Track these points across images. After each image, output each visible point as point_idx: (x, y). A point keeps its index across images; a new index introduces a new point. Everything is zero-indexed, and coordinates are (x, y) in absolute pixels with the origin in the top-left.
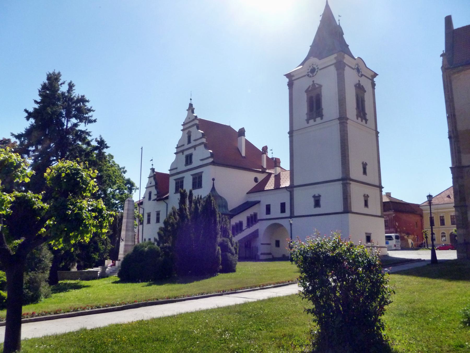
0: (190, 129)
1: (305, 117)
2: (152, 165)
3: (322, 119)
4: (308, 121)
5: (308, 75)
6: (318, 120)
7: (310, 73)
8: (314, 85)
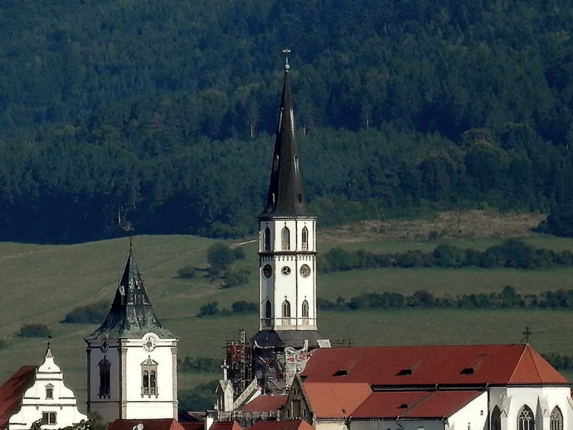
0: (52, 382)
1: (140, 391)
3: (157, 398)
4: (142, 396)
6: (153, 398)
7: (146, 346)
8: (149, 360)
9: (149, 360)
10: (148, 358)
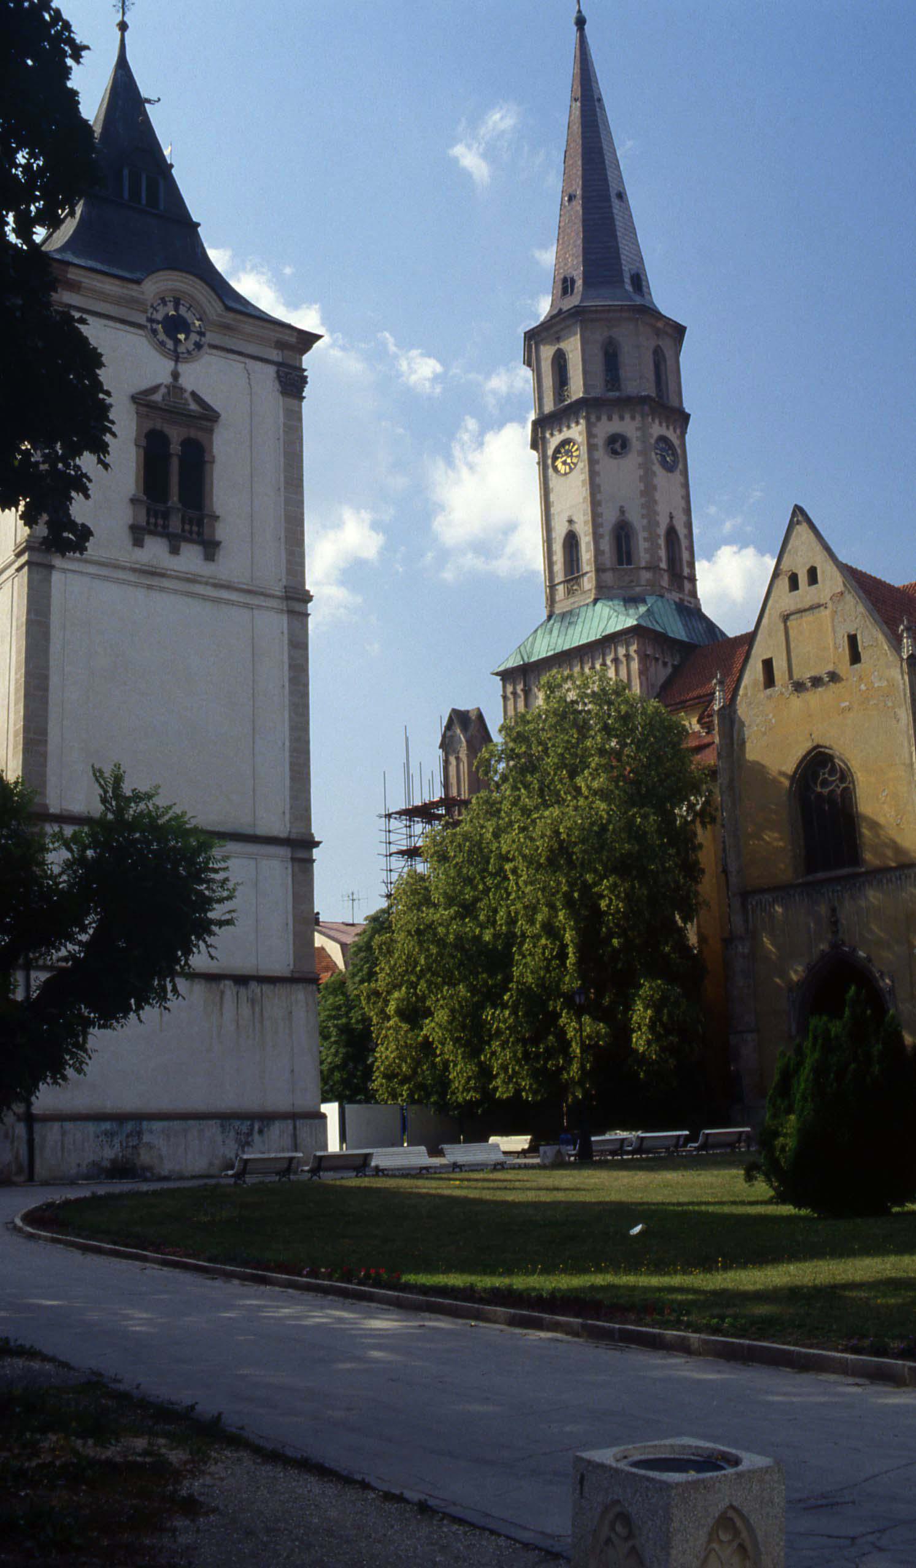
5: (154, 332)
6: (190, 559)
9: (175, 388)
10: (167, 380)
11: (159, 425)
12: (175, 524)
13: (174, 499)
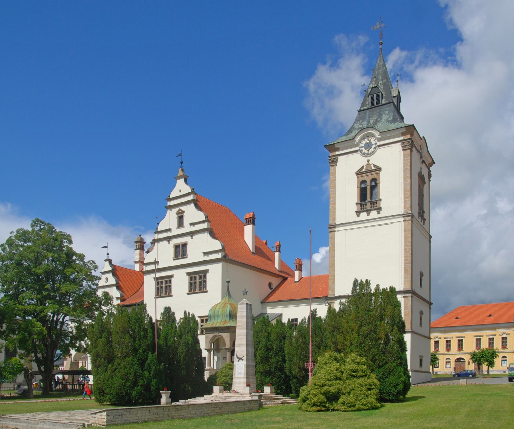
0: (183, 208)
1: (355, 208)
2: (108, 254)
4: (358, 213)
6: (374, 214)
7: (363, 149)
8: (368, 165)
9: (368, 165)
11: (363, 179)
12: (368, 206)
13: (368, 199)
